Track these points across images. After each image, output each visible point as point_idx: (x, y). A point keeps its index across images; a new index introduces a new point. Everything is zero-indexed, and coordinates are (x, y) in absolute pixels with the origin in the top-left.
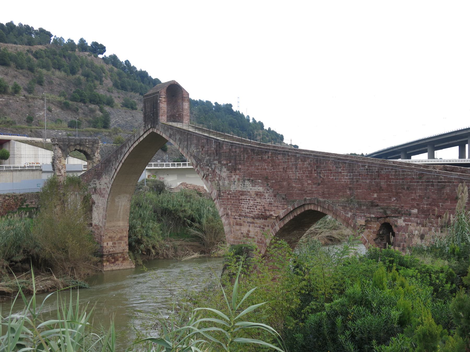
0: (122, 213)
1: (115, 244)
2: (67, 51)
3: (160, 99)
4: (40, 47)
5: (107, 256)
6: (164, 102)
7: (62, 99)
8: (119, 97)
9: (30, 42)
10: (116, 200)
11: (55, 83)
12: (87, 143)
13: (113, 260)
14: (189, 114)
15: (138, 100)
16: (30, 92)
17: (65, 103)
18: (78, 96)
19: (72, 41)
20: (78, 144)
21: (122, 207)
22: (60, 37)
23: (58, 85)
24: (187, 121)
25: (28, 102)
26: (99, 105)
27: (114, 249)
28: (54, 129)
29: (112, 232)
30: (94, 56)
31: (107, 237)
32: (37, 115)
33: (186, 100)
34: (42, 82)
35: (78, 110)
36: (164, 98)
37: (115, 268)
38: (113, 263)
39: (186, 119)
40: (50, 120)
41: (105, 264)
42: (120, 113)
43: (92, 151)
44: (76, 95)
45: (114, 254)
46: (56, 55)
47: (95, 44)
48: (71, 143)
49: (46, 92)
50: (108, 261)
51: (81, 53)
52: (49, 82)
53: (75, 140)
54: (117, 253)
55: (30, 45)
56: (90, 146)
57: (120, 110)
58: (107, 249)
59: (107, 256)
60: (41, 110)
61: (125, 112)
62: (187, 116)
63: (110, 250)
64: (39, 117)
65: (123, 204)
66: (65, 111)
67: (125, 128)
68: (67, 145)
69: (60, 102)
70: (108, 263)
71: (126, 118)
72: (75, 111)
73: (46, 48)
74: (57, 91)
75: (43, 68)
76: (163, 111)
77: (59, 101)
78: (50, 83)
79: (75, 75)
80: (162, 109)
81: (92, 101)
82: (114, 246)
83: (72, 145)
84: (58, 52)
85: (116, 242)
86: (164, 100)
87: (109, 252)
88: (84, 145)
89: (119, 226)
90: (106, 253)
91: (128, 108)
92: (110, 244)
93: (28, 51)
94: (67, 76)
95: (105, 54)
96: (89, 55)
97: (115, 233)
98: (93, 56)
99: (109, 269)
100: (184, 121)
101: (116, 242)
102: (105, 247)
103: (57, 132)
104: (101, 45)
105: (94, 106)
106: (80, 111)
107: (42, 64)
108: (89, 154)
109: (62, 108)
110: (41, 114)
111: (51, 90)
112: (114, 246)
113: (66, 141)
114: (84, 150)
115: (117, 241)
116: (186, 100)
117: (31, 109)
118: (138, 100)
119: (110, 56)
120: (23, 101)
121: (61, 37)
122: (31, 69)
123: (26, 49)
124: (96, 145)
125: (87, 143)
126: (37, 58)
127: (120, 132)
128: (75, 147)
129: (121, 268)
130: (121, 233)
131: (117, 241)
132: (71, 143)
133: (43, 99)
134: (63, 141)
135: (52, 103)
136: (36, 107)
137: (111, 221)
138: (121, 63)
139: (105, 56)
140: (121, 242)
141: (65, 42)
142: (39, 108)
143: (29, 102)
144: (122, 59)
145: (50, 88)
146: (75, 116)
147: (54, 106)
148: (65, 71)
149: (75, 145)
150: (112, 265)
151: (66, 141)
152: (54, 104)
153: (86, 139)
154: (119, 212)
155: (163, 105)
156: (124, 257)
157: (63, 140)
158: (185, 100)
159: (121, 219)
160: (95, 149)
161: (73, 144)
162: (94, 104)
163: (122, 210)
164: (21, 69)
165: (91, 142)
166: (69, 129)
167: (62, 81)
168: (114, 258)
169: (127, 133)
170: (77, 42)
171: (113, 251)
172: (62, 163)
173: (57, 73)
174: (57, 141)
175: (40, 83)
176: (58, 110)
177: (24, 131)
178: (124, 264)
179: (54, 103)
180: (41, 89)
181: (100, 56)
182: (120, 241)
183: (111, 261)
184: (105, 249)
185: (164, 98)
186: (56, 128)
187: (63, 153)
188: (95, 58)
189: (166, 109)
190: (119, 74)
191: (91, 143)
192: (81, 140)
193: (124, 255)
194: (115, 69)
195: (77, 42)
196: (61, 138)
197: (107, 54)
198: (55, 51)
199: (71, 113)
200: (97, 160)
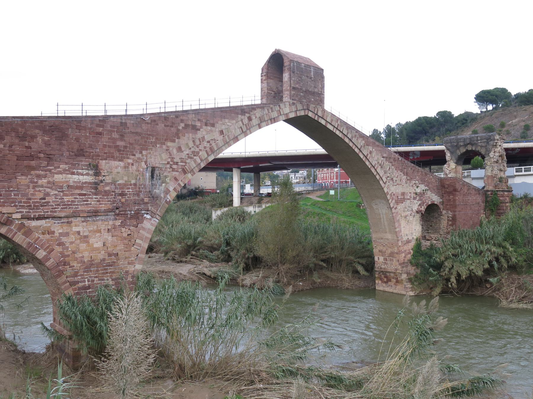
0: (386, 223)
1: (386, 260)
5: (379, 273)
10: (375, 207)
12: (479, 142)
13: (385, 280)
20: (468, 144)
29: (381, 246)
31: (377, 251)
33: (286, 69)
36: (265, 75)
37: (387, 289)
38: (386, 282)
41: (377, 282)
43: (487, 150)
45: (387, 272)
48: (460, 143)
50: (381, 279)
53: (464, 139)
54: (390, 272)
56: (484, 145)
58: (378, 265)
59: (379, 273)
63: (382, 267)
65: (384, 211)
68: (456, 146)
70: (380, 282)
82: (385, 263)
83: (461, 146)
87: (381, 268)
88: (476, 144)
89: (388, 239)
92: (382, 259)
99: (381, 288)
108: (484, 154)
112: (385, 263)
114: (477, 150)
115: (388, 257)
116: (286, 69)
124: (491, 143)
125: (479, 142)
129: (395, 291)
130: (390, 247)
134: (451, 143)
140: (393, 259)
149: (465, 145)
150: (384, 285)
153: (477, 137)
156: (397, 278)
159: (387, 230)
160: (490, 147)
161: (462, 144)
163: (385, 219)
165: (485, 139)
168: (386, 277)
171: (385, 269)
178: (398, 287)
182: (392, 258)
183: (384, 279)
184: (377, 264)
189: (266, 89)
191: (485, 140)
193: (396, 276)
200: (493, 161)
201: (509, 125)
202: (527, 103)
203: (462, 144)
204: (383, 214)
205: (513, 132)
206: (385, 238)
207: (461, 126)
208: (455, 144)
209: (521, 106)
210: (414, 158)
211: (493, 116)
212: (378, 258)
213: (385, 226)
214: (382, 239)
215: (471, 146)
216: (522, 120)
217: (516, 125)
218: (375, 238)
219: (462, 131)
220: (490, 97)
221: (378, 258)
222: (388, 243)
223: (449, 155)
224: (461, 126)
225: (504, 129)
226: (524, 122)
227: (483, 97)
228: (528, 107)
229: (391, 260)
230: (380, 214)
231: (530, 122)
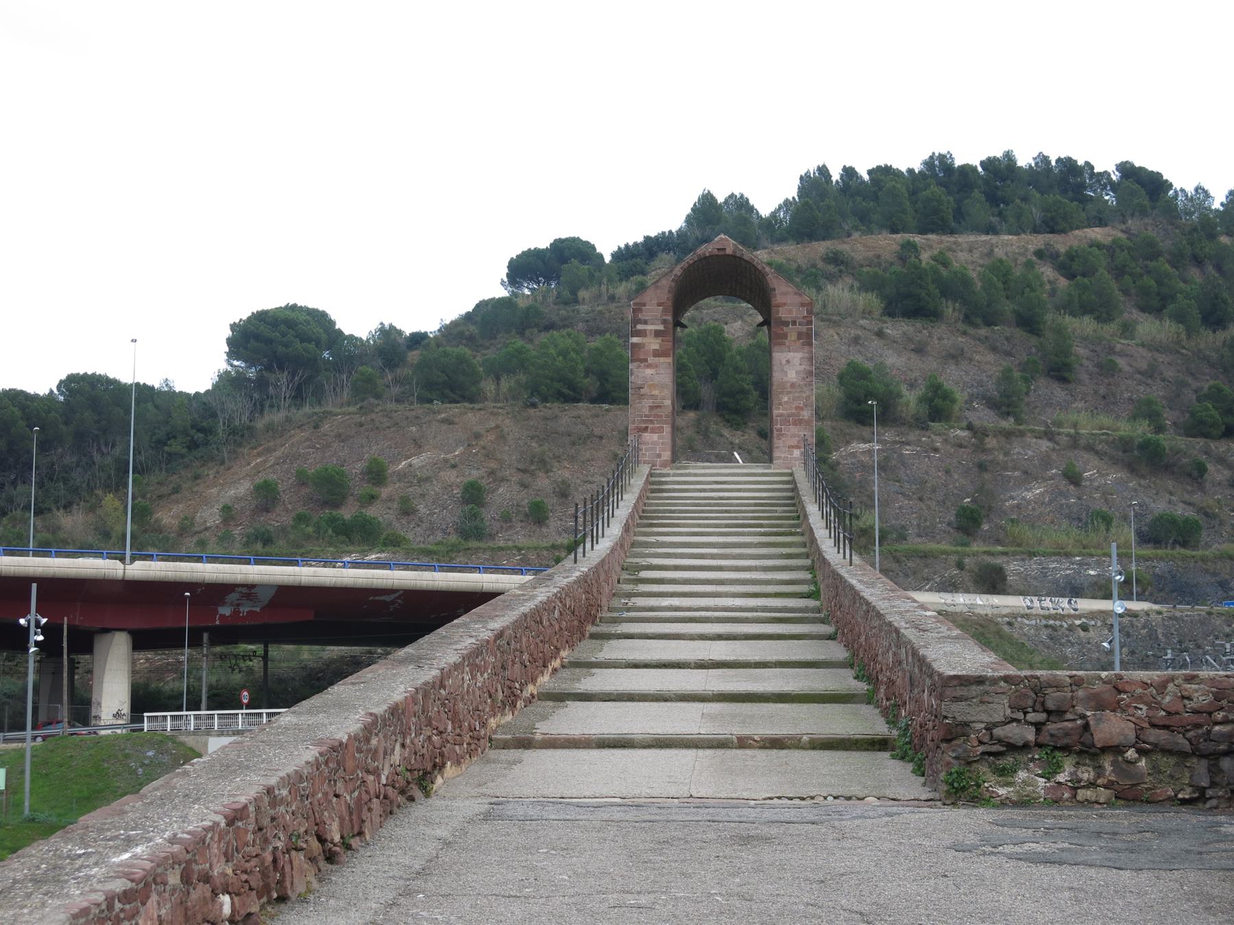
3: (635, 340)
4: (1097, 234)
6: (657, 354)
7: (1141, 430)
9: (1052, 219)
11: (1127, 368)
14: (806, 414)
16: (1004, 409)
17: (1145, 446)
18: (1214, 413)
19: (1207, 194)
22: (1190, 190)
24: (797, 453)
25: (980, 448)
28: (1068, 555)
32: (1012, 498)
33: (793, 336)
34: (1067, 367)
35: (1201, 469)
36: (657, 334)
39: (794, 442)
40: (1068, 516)
44: (1207, 409)
46: (1155, 255)
49: (1080, 405)
52: (1100, 366)
55: (1052, 231)
60: (1036, 479)
62: (798, 422)
64: (1018, 506)
66: (1143, 477)
69: (1125, 445)
72: (1190, 475)
73: (1120, 235)
74: (1130, 399)
75: (1084, 314)
76: (647, 403)
77: (1121, 439)
78: (1107, 369)
80: (641, 397)
84: (1166, 245)
86: (654, 344)
93: (1039, 254)
94: (1189, 337)
103: (1081, 564)
107: (1080, 296)
109: (1132, 468)
110: (1029, 495)
111: (1104, 397)
116: (793, 336)
117: (987, 476)
120: (961, 446)
122: (1029, 323)
123: (1032, 248)
126: (1071, 276)
133: (1049, 435)
135: (1090, 448)
136: (1014, 469)
142: (1026, 472)
143: (984, 451)
145: (1102, 391)
146: (1187, 497)
147: (1094, 461)
148: (1180, 318)
152: (1097, 453)
155: (649, 372)
158: (785, 336)
164: (989, 323)
166: (1148, 551)
167: (1161, 358)
173: (1148, 327)
175: (1060, 372)
176: (1114, 476)
177: (927, 566)
180: (1059, 393)
185: (657, 334)
186: (1076, 551)
198: (1151, 244)
199: (1170, 484)
201: (401, 476)
202: (447, 391)
205: (422, 509)
207: (183, 456)
209: (430, 401)
210: (236, 613)
211: (326, 427)
216: (446, 461)
217: (428, 479)
219: (197, 477)
220: (298, 345)
224: (183, 456)
225: (385, 492)
226: (454, 472)
227: (269, 341)
228: (454, 410)
231: (475, 473)
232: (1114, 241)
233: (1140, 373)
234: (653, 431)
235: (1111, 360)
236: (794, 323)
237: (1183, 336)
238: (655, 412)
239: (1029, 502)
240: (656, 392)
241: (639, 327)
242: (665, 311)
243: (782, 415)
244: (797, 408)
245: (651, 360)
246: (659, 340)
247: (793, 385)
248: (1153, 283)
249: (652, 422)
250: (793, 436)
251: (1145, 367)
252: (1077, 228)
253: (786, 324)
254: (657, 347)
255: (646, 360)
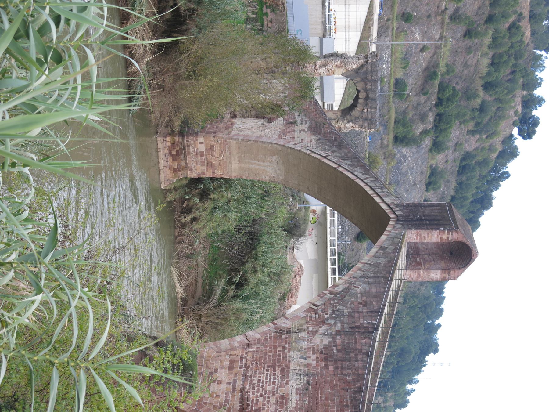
2: (523, 77)
3: (446, 232)
4: (528, 33)
5: (181, 143)
6: (441, 238)
7: (442, 69)
8: (447, 162)
9: (536, 17)
10: (274, 158)
11: (468, 57)
12: (369, 110)
13: (174, 152)
14: (420, 279)
15: (443, 192)
16: (453, 17)
17: (435, 73)
18: (448, 95)
19: (540, 85)
20: (368, 95)
21: (262, 168)
23: (466, 63)
24: (408, 277)
25: (437, 14)
26: (432, 128)
27: (194, 154)
28: (391, 56)
29: (220, 150)
30: (515, 121)
31: (213, 143)
32: (416, 29)
33: (445, 275)
34: (470, 37)
35: (425, 94)
36: (448, 238)
37: (161, 155)
38: (170, 153)
39: (412, 276)
40: (407, 50)
41: (168, 139)
42: (420, 163)
43: (357, 118)
44: (449, 92)
45: (185, 154)
46: (516, 59)
47: (536, 122)
48: (369, 84)
49: (454, 43)
50: (173, 144)
51: (520, 98)
52: (470, 47)
53: (375, 91)
54: (185, 160)
55: (530, 17)
56: (364, 115)
57: (425, 163)
58: (192, 142)
59: (181, 143)
60: (423, 36)
61: (422, 172)
62: (418, 277)
64: (412, 32)
65: (268, 169)
66: (423, 73)
67: (396, 172)
68: (366, 78)
69: (437, 66)
70: (169, 144)
71: (412, 174)
72: (422, 90)
73: (526, 42)
74: (455, 60)
75: (492, 38)
76: (426, 235)
77: (439, 64)
78: (469, 50)
79: (483, 90)
80: (428, 234)
81: (439, 117)
83: (366, 85)
84: (521, 62)
85: (205, 157)
86: (445, 237)
87: (189, 146)
88: (366, 105)
89: (230, 163)
90: (187, 141)
91: (429, 177)
92: (202, 148)
93: (521, 14)
94: (480, 77)
95: (520, 138)
96: (516, 112)
97: (220, 155)
98: (516, 118)
99: (160, 146)
100: (408, 271)
101: (205, 157)
102: (197, 140)
103: (388, 61)
104: (534, 132)
105: (432, 121)
106: (423, 99)
107: (500, 37)
108: (352, 114)
109: (427, 69)
110: (416, 35)
111: (457, 51)
112: (197, 154)
113: (372, 76)
114: (358, 105)
115: (207, 159)
116: (445, 275)
117: (425, 19)
118: (443, 192)
119: (516, 147)
120: (438, 7)
121: (545, 67)
122: (490, 19)
123: (523, 11)
124: (366, 124)
125: (369, 110)
126: (509, 29)
127: (388, 164)
128: (362, 91)
129: (161, 166)
130: (220, 165)
131: (207, 159)
132: (369, 84)
133: (441, 38)
134: (372, 71)
135: (435, 53)
136: (428, 28)
137: (239, 148)
138: (505, 165)
139: (516, 138)
140: (203, 165)
141: (537, 73)
142: (426, 32)
143: (436, 16)
144: (512, 167)
145: (459, 50)
146: (414, 89)
147: (429, 56)
148: (489, 74)
149: (366, 91)
150: (166, 150)
151: (372, 76)
152: (433, 56)
153: (376, 108)
154: (255, 162)
155: (436, 236)
156: (180, 171)
157: (375, 71)
158: (445, 273)
159: (243, 165)
160: (360, 123)
161: (368, 87)
162: (435, 121)
163: (258, 167)
164: (491, 4)
165: (372, 117)
166: (393, 81)
167: (472, 69)
168: (178, 154)
169: (386, 175)
170: (537, 92)
171: (189, 152)
172: (336, 69)
173: (486, 61)
174: (372, 62)
175: (468, 34)
176: (423, 63)
177: (388, 8)
178: (168, 170)
179: (435, 56)
180: (459, 35)
181: (515, 131)
182: (205, 164)
183: (174, 150)
184: (193, 140)
185: (448, 238)
186: (393, 59)
187: (352, 70)
188: (512, 121)
189: (429, 241)
190: (485, 162)
192: (374, 100)
193: (183, 170)
194: (494, 156)
195: (537, 92)
196: (378, 68)
197: (519, 142)
198: (521, 57)
199: (419, 83)
200: (342, 127)
203: (368, 87)
204: (265, 166)
206: (232, 158)
208: (369, 77)
212: (202, 143)
213: (249, 163)
214: (230, 154)
215: (364, 97)
218: (230, 143)
221: (202, 143)
222: (225, 162)
223: (354, 67)
229: (203, 162)
230: (264, 161)
232: (524, 42)
233: (466, 62)
234: (417, 237)
235: (472, 52)
236: (449, 276)
237: (481, 75)
238: (423, 237)
239: (414, 35)
240: (429, 238)
241: (450, 233)
242: (455, 239)
243: (420, 272)
244: (422, 277)
245: (440, 236)
246: (446, 238)
247: (429, 276)
248: (504, 60)
249: (420, 237)
250: (414, 276)
251: (469, 63)
252: (531, 26)
253: (449, 274)
254: (444, 238)
255: (440, 235)
